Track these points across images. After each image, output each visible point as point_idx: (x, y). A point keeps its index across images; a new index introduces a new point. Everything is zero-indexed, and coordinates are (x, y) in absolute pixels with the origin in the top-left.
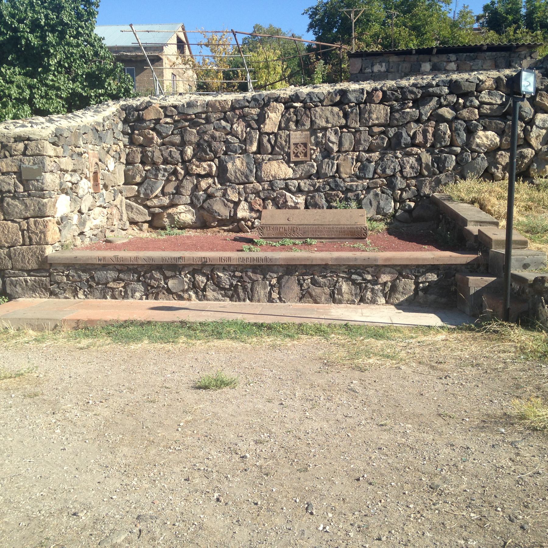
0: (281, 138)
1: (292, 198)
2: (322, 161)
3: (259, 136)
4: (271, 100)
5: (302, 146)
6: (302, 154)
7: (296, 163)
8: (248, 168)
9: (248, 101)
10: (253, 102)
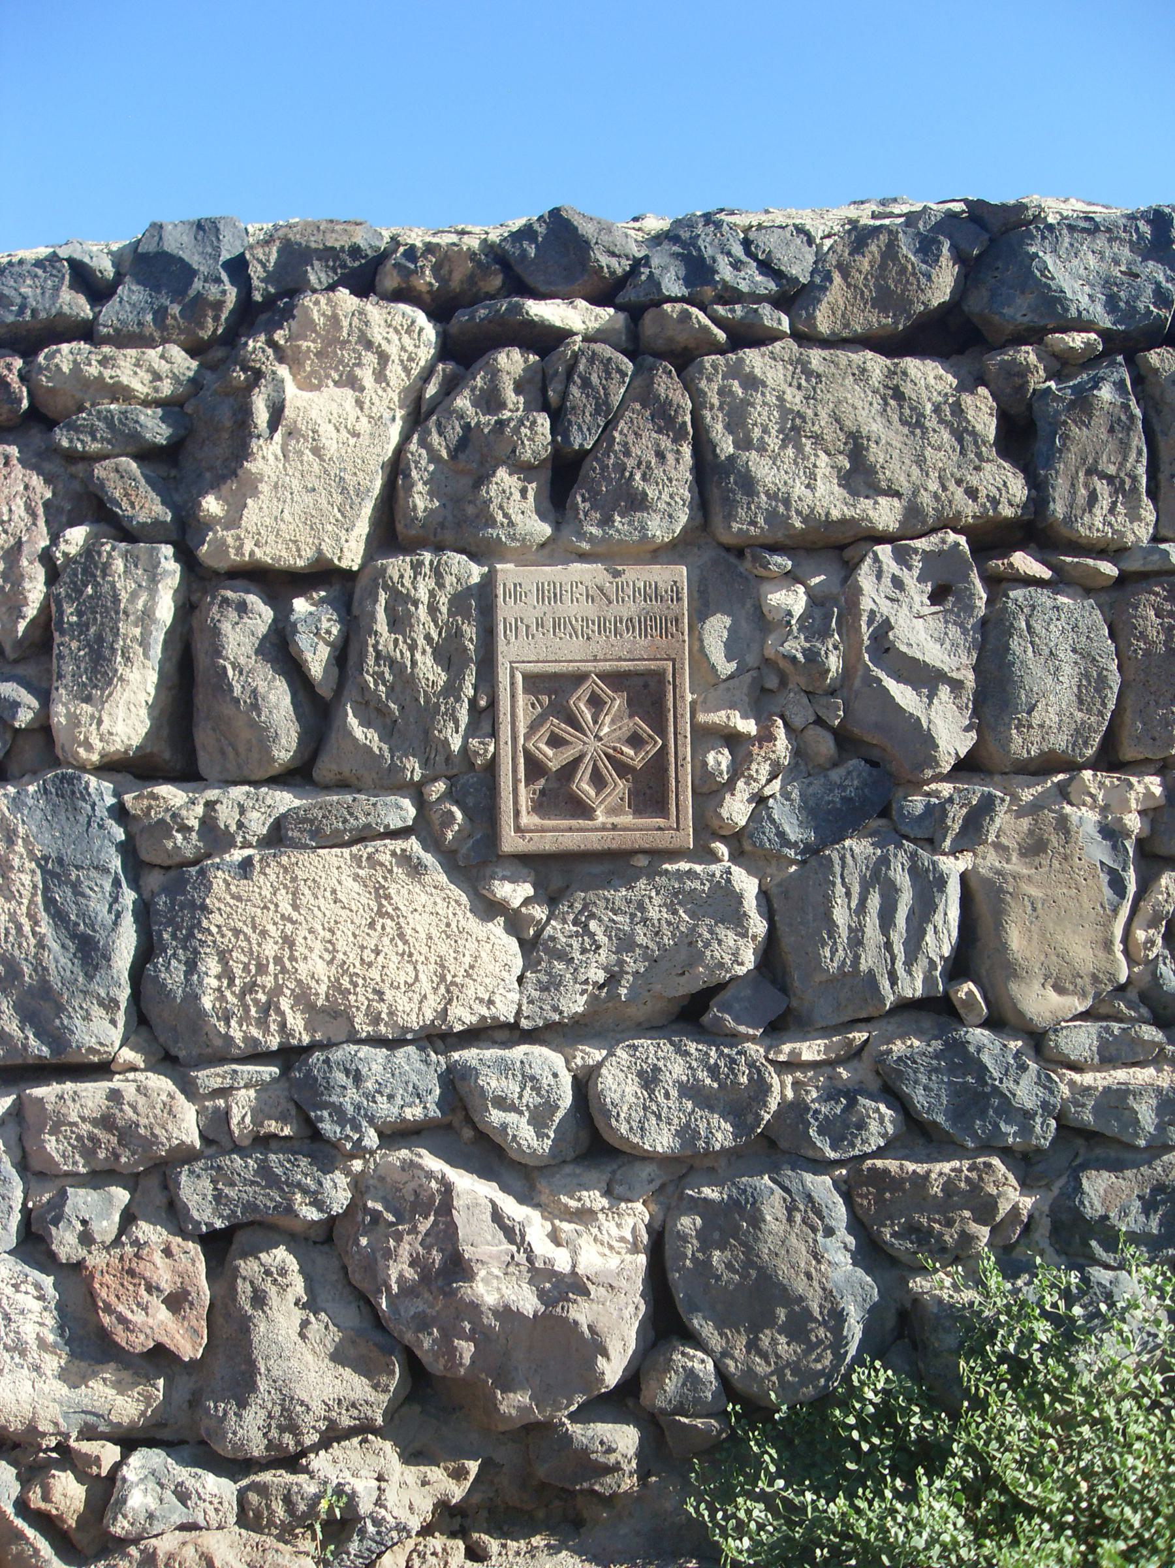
0: (399, 622)
1: (511, 1233)
2: (812, 852)
3: (187, 608)
4: (316, 275)
5: (617, 702)
6: (620, 787)
7: (557, 875)
8: (58, 916)
9: (82, 277)
10: (131, 293)
